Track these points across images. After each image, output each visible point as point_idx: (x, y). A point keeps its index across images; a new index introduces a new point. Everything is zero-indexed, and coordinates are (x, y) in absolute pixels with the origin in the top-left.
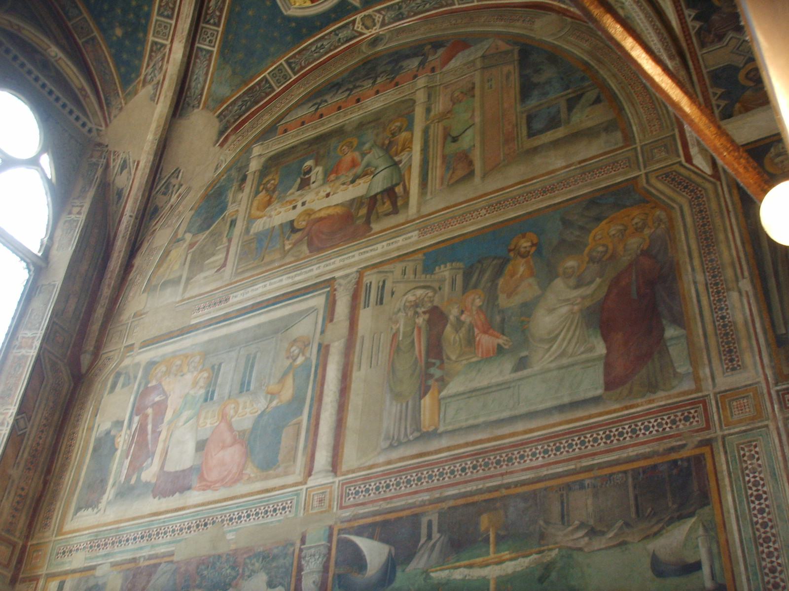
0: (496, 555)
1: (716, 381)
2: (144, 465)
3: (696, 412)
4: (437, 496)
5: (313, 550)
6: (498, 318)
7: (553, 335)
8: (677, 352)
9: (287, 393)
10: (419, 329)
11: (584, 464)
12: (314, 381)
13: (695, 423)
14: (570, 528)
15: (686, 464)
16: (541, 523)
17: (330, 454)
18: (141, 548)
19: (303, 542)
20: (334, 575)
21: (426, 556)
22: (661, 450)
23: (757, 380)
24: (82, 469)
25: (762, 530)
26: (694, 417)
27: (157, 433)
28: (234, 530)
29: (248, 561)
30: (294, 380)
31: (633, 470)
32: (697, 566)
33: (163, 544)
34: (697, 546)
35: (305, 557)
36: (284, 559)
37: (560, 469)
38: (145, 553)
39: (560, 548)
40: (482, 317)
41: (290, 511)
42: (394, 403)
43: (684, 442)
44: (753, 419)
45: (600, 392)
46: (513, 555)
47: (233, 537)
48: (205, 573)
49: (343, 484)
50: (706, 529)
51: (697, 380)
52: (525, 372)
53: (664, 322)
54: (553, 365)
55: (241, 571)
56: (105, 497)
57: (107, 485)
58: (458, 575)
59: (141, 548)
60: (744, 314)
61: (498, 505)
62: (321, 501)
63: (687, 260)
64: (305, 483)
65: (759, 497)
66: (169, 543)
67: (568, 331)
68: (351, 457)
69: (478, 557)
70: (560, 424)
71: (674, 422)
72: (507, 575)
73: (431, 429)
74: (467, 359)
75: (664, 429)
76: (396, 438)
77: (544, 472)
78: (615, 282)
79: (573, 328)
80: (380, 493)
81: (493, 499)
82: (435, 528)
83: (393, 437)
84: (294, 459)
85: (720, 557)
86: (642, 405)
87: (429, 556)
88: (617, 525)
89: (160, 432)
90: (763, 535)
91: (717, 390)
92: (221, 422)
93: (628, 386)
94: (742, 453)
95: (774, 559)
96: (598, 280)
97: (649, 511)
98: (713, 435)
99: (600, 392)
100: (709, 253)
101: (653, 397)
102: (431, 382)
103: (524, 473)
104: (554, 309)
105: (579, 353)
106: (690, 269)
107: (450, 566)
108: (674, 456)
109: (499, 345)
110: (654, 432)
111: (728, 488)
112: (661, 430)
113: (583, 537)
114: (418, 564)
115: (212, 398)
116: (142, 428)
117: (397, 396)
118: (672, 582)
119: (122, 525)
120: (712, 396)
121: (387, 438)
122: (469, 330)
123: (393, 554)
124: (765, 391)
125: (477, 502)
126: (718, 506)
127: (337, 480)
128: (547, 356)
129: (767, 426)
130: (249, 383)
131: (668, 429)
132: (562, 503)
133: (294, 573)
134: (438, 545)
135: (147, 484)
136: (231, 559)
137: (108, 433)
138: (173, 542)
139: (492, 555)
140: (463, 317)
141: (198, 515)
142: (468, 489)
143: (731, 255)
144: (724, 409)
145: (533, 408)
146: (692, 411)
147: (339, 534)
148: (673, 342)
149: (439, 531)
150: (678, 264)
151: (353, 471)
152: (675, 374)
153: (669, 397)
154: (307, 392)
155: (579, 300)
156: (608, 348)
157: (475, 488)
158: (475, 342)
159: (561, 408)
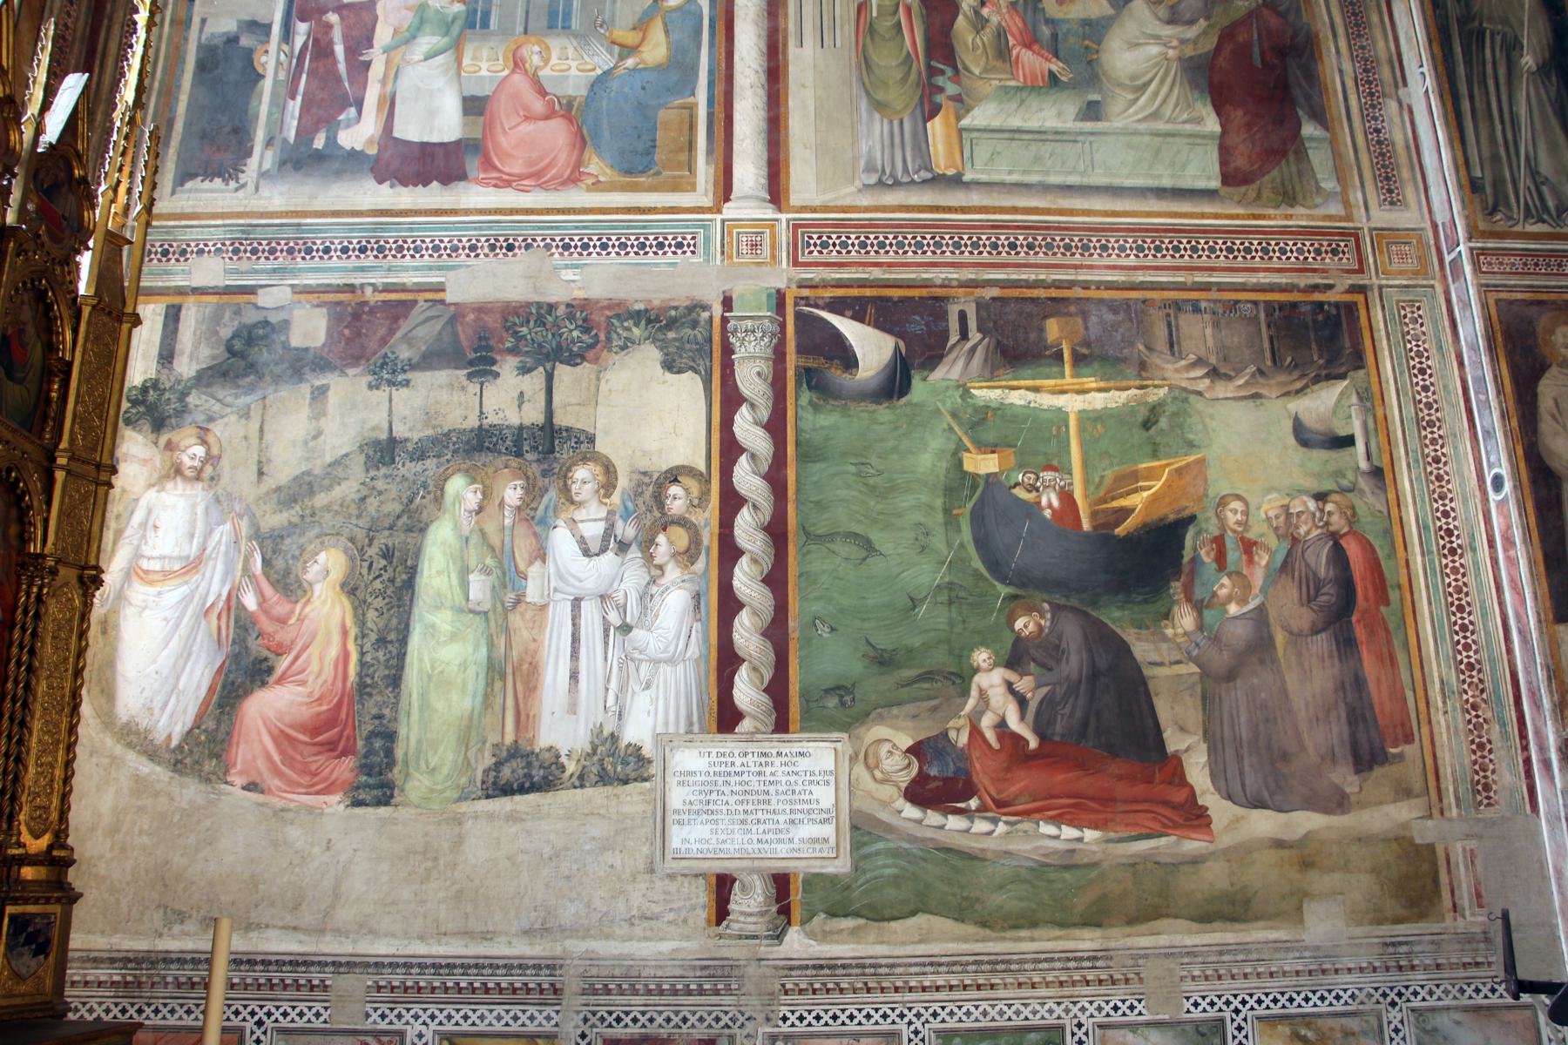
0: (1075, 380)
1: (1371, 212)
2: (342, 117)
3: (1346, 246)
4: (973, 276)
5: (749, 323)
6: (1046, 31)
7: (1139, 82)
8: (1319, 158)
9: (656, 49)
10: (909, 10)
11: (1196, 279)
12: (711, 45)
13: (1344, 261)
14: (1183, 363)
15: (1334, 311)
16: (1141, 347)
17: (764, 172)
18: (362, 269)
19: (727, 303)
20: (797, 367)
21: (961, 363)
22: (1302, 285)
23: (1422, 225)
24: (177, 99)
25: (1426, 412)
26: (1344, 253)
27: (360, 69)
28: (577, 266)
29: (615, 322)
30: (667, 32)
31: (1265, 302)
32: (1349, 441)
33: (416, 269)
34: (1350, 417)
35: (736, 330)
36: (694, 328)
37: (1163, 278)
38: (378, 279)
39: (1171, 387)
40: (1017, 20)
41: (693, 252)
42: (877, 116)
43: (1331, 282)
44: (1416, 273)
45: (1215, 184)
46: (1102, 384)
47: (576, 278)
48: (524, 330)
49: (796, 227)
50: (1361, 399)
51: (1346, 204)
52: (1099, 126)
53: (1301, 113)
54: (1142, 127)
55: (602, 337)
56: (253, 163)
57: (251, 140)
58: (1017, 398)
59: (362, 269)
60: (1405, 134)
61: (1072, 309)
62: (754, 246)
63: (1331, 37)
64: (719, 211)
65: (1422, 371)
66: (430, 268)
67: (1162, 81)
68: (804, 184)
69: (1048, 377)
70: (1159, 215)
71: (1318, 252)
72: (1094, 411)
73: (951, 172)
74: (1000, 80)
75: (1306, 258)
76: (888, 172)
77: (1140, 277)
78: (1227, 35)
79: (1169, 80)
80: (868, 252)
81: (1063, 299)
82: (972, 324)
83: (883, 171)
84: (691, 166)
85: (1377, 436)
86: (1275, 218)
87: (967, 364)
88: (1248, 371)
89: (368, 65)
90: (1427, 418)
91: (1373, 225)
92: (513, 71)
93: (1255, 186)
94: (1403, 313)
95: (1438, 447)
96: (1202, 23)
97: (1289, 359)
98: (1366, 282)
99: (1215, 184)
100: (1359, 36)
101: (1290, 211)
102: (939, 98)
103: (1110, 272)
104: (1137, 45)
105: (1180, 120)
106: (1333, 51)
107: (1003, 383)
108: (1318, 297)
109: (1050, 72)
110: (1293, 259)
111: (1387, 353)
112: (1301, 258)
113: (1201, 378)
114: (949, 371)
115: (485, 24)
116: (321, 48)
117: (878, 106)
118: (1320, 455)
119: (309, 221)
120: (1366, 230)
121: (870, 169)
122: (999, 34)
123: (904, 352)
124: (1432, 242)
125: (1038, 298)
126: (1373, 372)
127: (783, 217)
128: (1131, 111)
129: (1432, 286)
130: (567, 16)
131: (1310, 260)
132: (1169, 325)
133: (717, 354)
134: (980, 350)
135: (354, 155)
136: (578, 315)
137: (232, 40)
138: (440, 268)
139: (1068, 380)
140: (985, 12)
141: (490, 228)
142: (1024, 277)
143: (1388, 48)
144: (1381, 252)
145: (1117, 182)
146: (1342, 244)
147: (796, 304)
148: (1313, 144)
149: (979, 330)
150: (1317, 36)
151: (814, 210)
152: (1319, 188)
153: (1312, 218)
154: (698, 57)
155: (1175, 43)
156: (1222, 126)
157: (1033, 277)
158: (1010, 56)
159: (1160, 193)
